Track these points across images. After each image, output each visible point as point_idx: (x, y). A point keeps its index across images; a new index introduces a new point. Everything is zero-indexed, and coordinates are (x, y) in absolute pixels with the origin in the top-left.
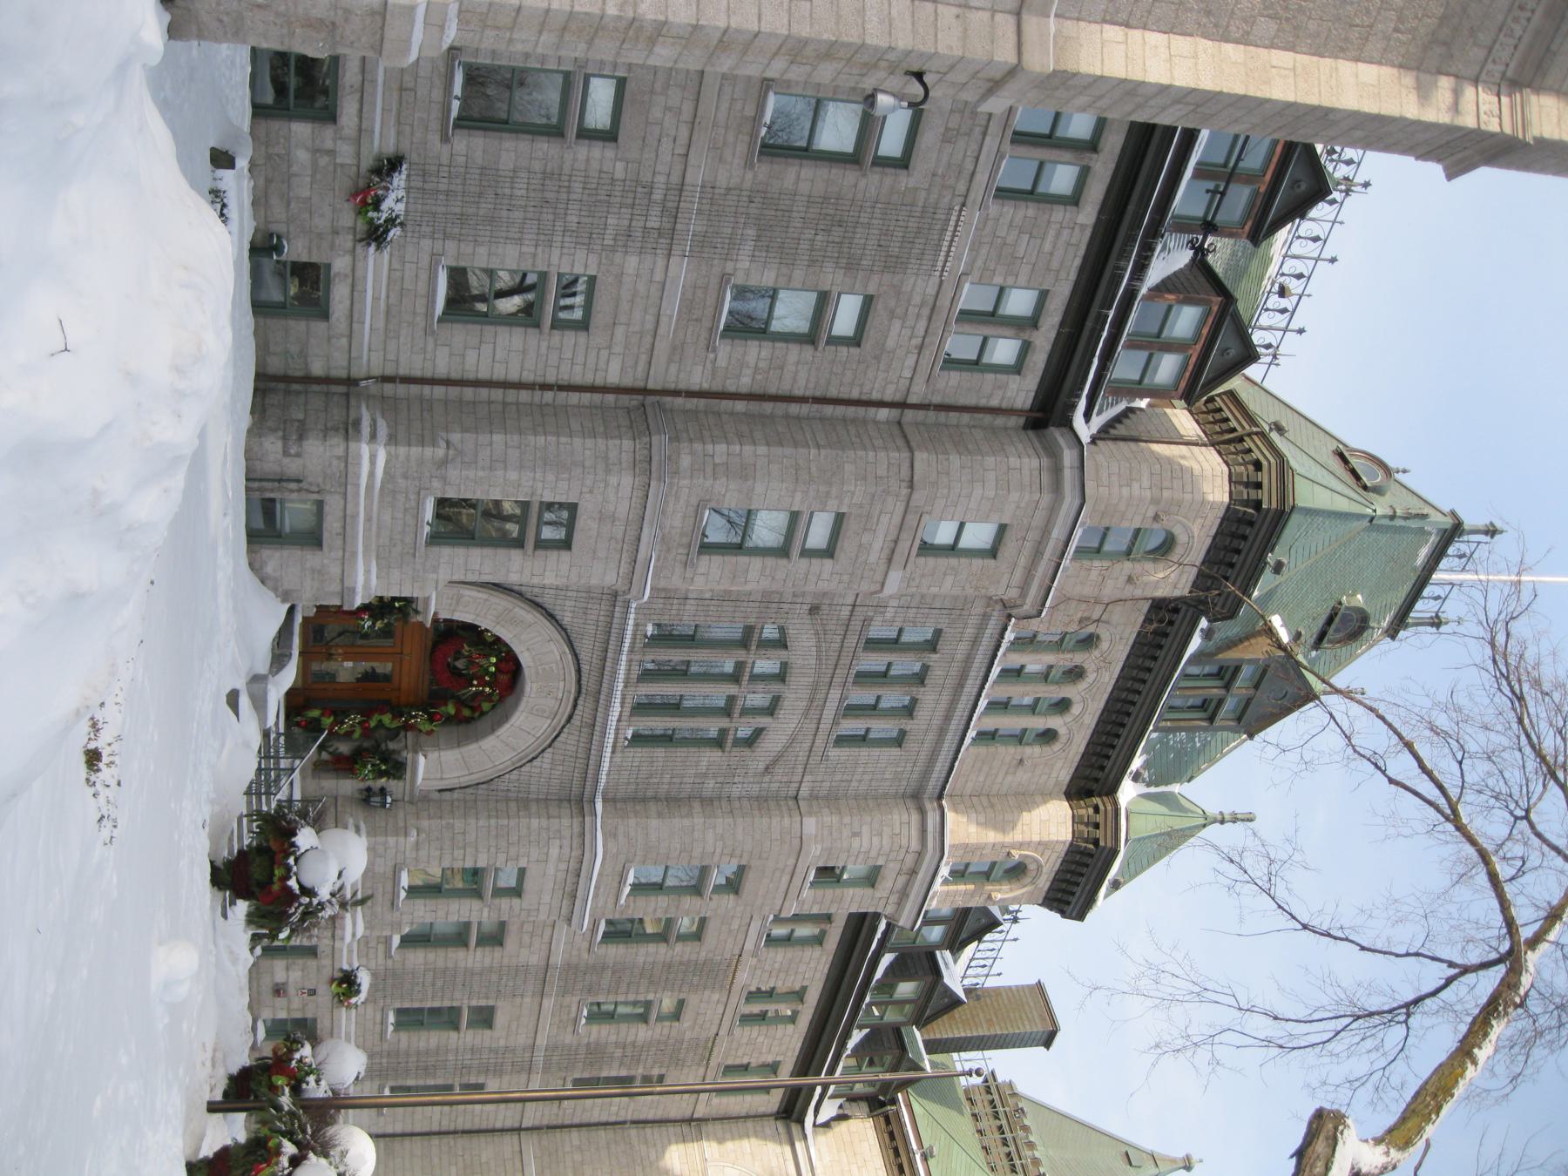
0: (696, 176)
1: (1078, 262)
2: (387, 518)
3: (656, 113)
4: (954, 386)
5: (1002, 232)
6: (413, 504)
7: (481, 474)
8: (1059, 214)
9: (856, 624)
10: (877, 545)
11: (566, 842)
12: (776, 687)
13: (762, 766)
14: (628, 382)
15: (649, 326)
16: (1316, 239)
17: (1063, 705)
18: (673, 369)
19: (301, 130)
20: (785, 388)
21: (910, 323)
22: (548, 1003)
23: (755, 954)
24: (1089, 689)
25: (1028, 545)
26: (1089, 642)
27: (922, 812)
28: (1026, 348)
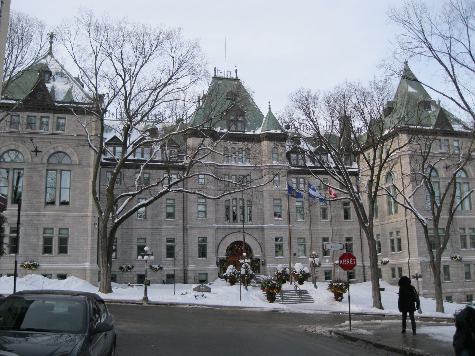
0: (149, 227)
14: (182, 232)
20: (182, 209)
22: (320, 227)
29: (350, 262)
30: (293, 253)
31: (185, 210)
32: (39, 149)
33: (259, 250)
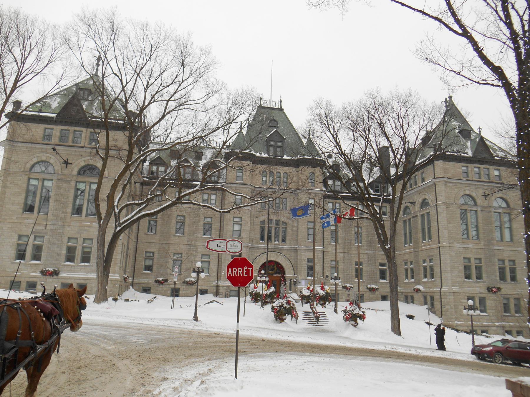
0: (186, 243)
19: (180, 292)
20: (219, 227)
29: (243, 273)
30: (325, 275)
31: (222, 229)
32: (69, 161)
33: (291, 270)
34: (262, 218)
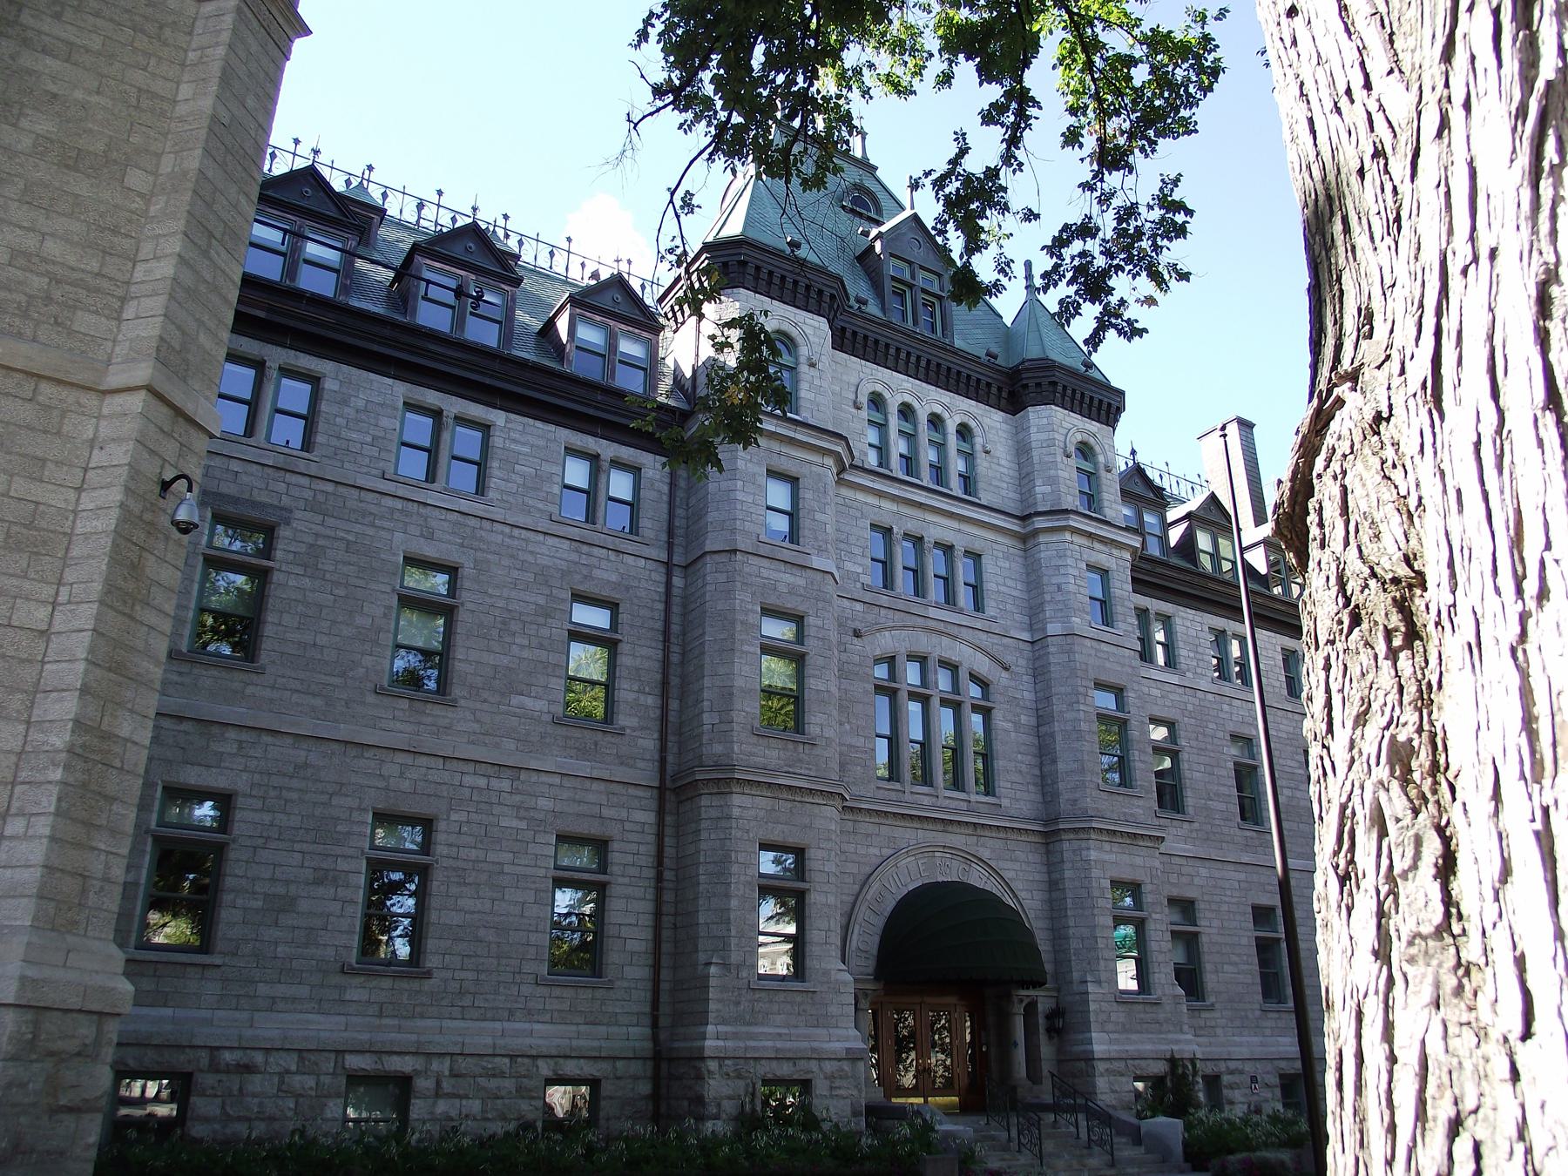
1: (539, 424)
2: (779, 1019)
3: (406, 785)
4: (651, 525)
5: (513, 487)
6: (763, 994)
7: (733, 933)
8: (497, 441)
9: (868, 597)
10: (787, 578)
11: (1084, 844)
12: (931, 664)
13: (1004, 674)
15: (602, 786)
16: (552, 254)
17: (936, 421)
18: (641, 764)
21: (594, 561)
23: (1183, 674)
24: (919, 399)
25: (785, 449)
26: (877, 401)
27: (1036, 532)
28: (617, 464)
34: (886, 642)
